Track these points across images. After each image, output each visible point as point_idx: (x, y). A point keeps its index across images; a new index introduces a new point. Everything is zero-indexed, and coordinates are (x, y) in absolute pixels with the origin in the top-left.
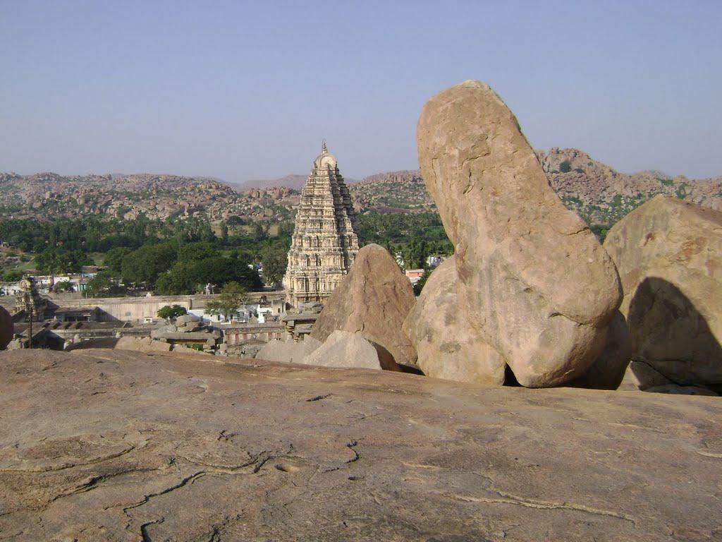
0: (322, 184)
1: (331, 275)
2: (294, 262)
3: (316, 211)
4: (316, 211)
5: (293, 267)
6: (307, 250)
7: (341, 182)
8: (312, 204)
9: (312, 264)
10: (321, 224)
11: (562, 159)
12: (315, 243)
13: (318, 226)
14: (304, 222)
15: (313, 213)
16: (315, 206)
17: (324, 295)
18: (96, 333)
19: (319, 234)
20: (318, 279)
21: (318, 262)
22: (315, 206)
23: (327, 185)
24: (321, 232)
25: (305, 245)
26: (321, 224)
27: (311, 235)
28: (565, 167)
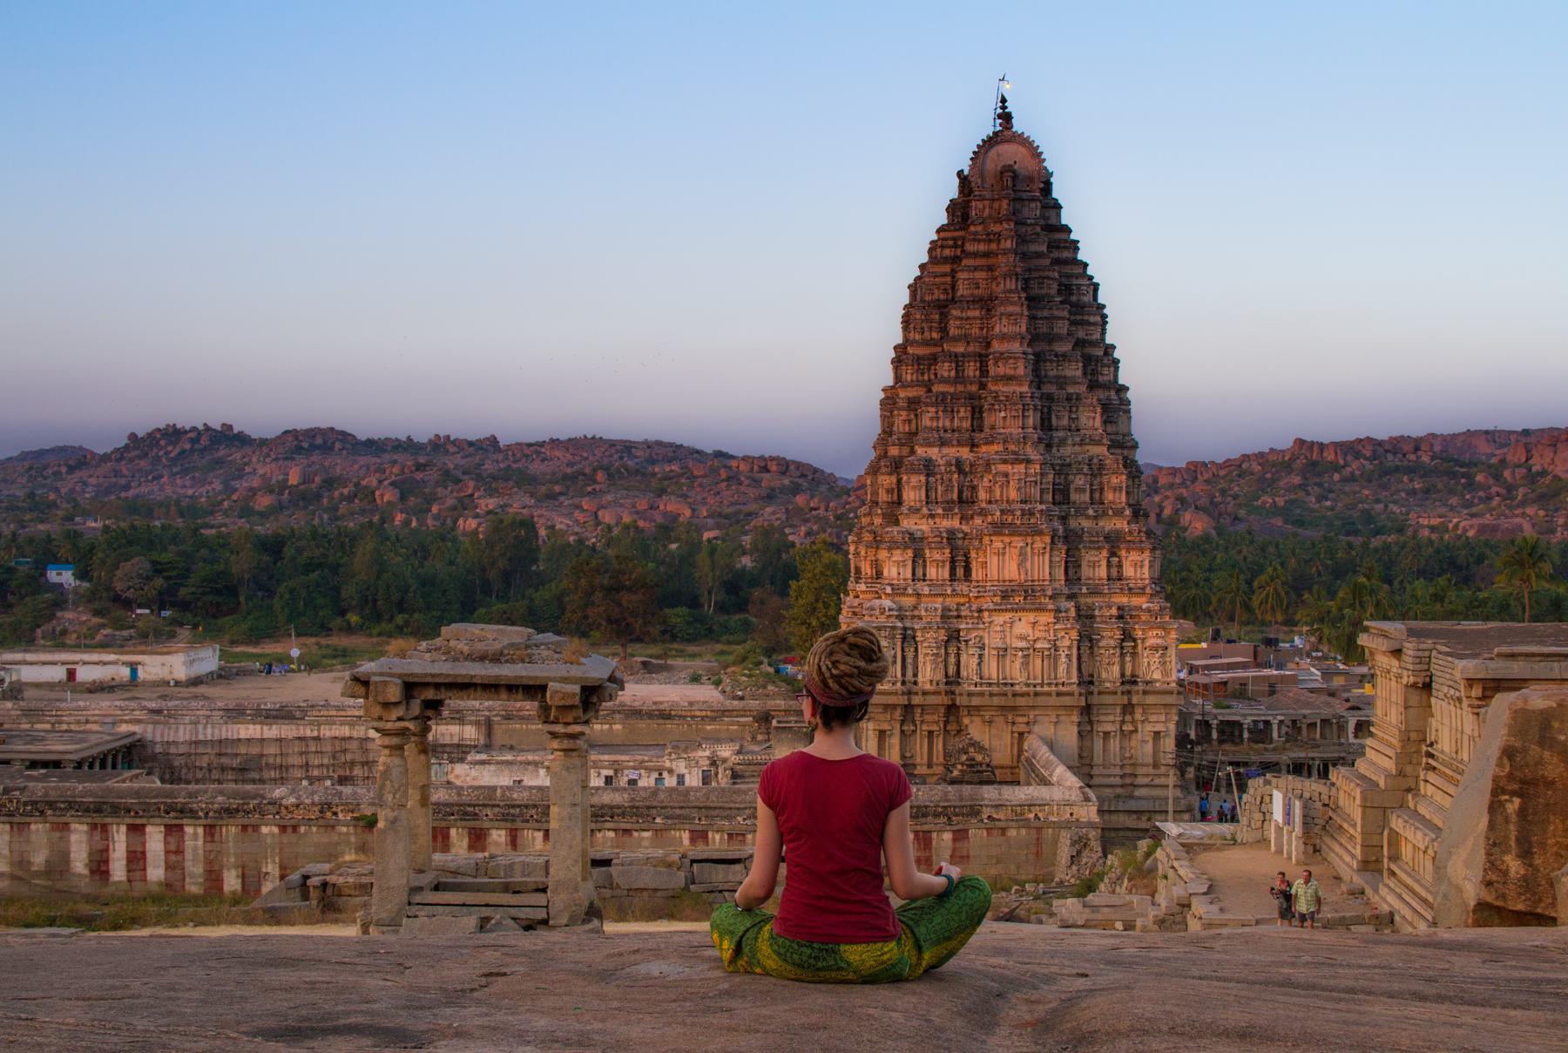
0: (986, 255)
1: (1007, 616)
2: (867, 569)
4: (957, 360)
5: (863, 587)
7: (1066, 254)
9: (932, 572)
10: (977, 413)
12: (949, 489)
13: (962, 419)
15: (945, 369)
17: (975, 701)
19: (965, 453)
21: (960, 566)
22: (956, 339)
23: (1005, 252)
24: (973, 446)
26: (977, 413)
27: (933, 452)
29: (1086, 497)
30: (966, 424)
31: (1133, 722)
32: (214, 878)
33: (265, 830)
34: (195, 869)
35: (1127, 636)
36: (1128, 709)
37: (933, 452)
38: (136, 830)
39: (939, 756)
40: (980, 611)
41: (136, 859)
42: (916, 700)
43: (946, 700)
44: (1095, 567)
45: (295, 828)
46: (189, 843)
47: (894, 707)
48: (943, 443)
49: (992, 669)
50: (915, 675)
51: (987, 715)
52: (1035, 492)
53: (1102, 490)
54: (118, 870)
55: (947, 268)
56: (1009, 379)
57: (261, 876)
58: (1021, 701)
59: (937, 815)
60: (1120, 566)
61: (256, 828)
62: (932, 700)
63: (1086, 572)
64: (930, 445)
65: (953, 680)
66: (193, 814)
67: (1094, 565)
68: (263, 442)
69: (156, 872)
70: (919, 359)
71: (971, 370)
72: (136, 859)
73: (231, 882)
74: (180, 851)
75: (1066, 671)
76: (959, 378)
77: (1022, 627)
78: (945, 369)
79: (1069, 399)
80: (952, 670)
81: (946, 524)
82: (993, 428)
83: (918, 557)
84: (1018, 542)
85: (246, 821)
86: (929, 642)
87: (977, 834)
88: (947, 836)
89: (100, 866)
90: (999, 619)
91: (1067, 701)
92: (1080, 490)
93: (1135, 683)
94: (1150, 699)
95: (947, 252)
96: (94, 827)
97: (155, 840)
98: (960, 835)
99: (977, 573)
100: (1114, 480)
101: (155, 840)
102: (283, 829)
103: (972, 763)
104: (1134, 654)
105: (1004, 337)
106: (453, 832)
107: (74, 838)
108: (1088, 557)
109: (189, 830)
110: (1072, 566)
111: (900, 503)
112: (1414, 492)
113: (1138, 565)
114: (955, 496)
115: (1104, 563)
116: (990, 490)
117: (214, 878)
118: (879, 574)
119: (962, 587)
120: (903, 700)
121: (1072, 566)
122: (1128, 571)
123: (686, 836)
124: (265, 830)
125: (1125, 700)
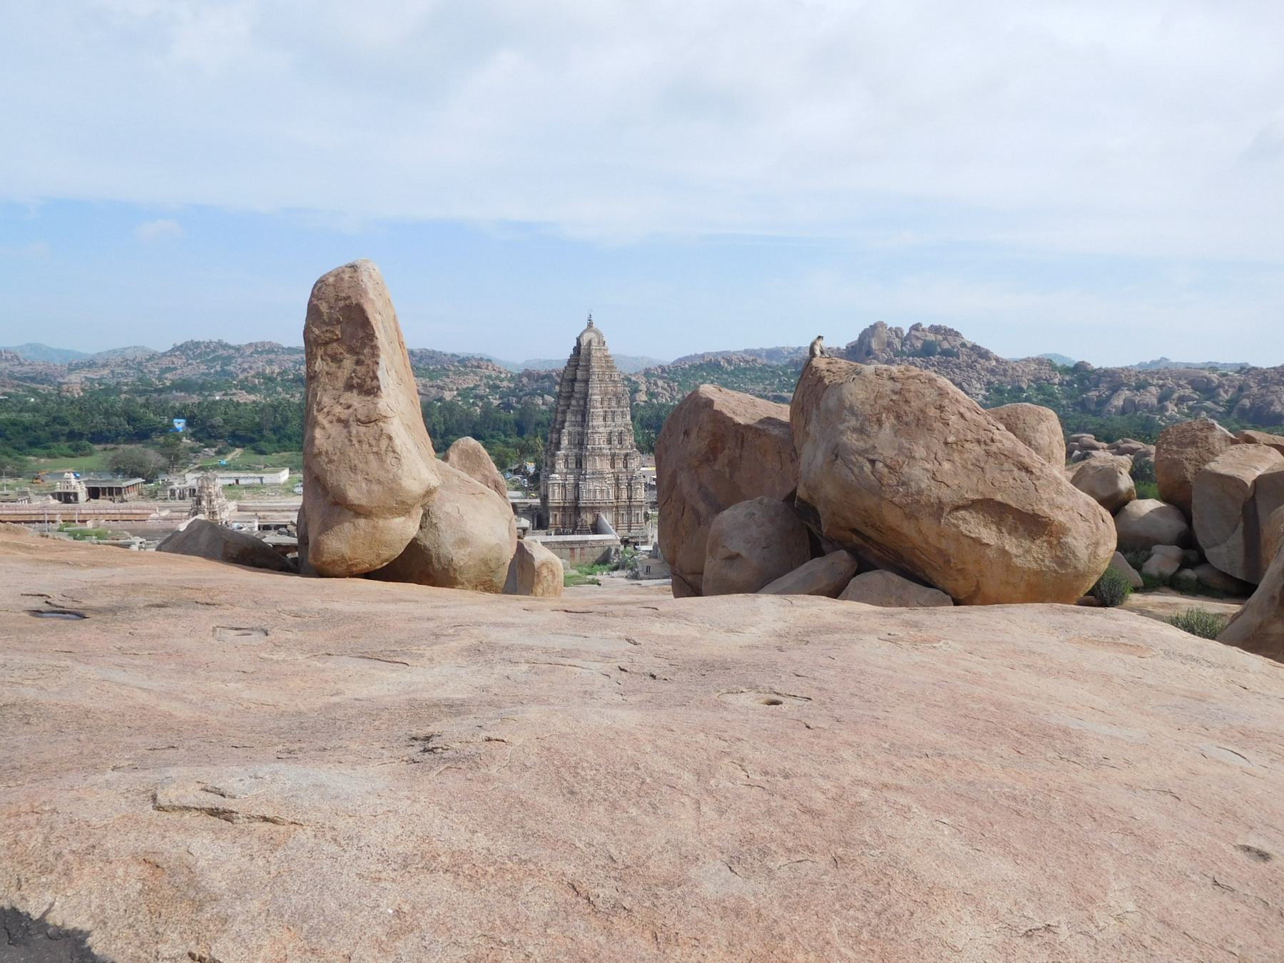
10: (583, 416)
13: (579, 418)
19: (580, 429)
21: (579, 463)
25: (565, 442)
26: (583, 416)
35: (630, 485)
36: (629, 507)
44: (620, 465)
65: (577, 498)
71: (582, 402)
75: (612, 497)
78: (574, 402)
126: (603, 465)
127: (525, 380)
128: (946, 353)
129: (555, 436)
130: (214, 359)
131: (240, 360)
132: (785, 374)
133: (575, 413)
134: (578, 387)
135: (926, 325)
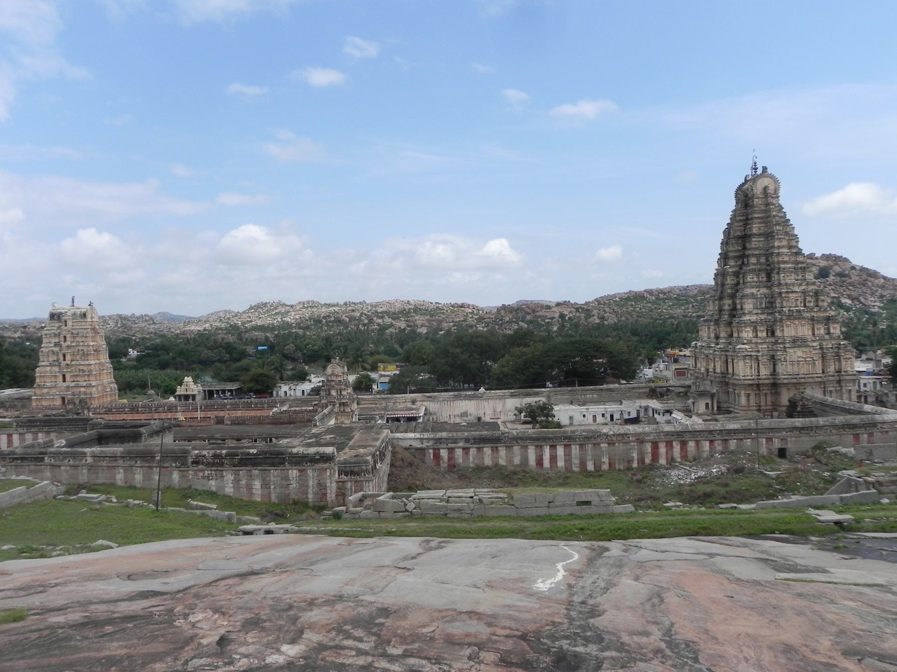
2: (723, 334)
3: (758, 256)
4: (758, 256)
6: (750, 313)
8: (745, 248)
9: (760, 334)
10: (769, 276)
11: (823, 263)
14: (736, 274)
16: (755, 249)
17: (785, 381)
18: (474, 439)
19: (765, 290)
20: (773, 357)
21: (772, 332)
25: (748, 306)
26: (769, 276)
27: (754, 291)
28: (823, 273)
29: (812, 304)
30: (765, 279)
31: (841, 386)
32: (583, 464)
33: (602, 445)
34: (576, 462)
36: (839, 382)
37: (754, 291)
38: (553, 447)
39: (769, 403)
40: (785, 347)
41: (553, 458)
42: (761, 382)
43: (772, 381)
45: (614, 444)
46: (573, 452)
47: (752, 385)
48: (759, 287)
49: (790, 369)
50: (759, 372)
51: (789, 386)
52: (799, 303)
53: (817, 301)
54: (546, 463)
55: (742, 224)
56: (784, 262)
57: (601, 463)
58: (803, 380)
59: (860, 427)
60: (828, 329)
61: (599, 444)
62: (767, 382)
63: (816, 332)
64: (752, 288)
65: (774, 373)
66: (574, 440)
67: (819, 329)
68: (292, 306)
69: (561, 463)
70: (736, 257)
71: (763, 260)
72: (553, 458)
73: (590, 467)
74: (570, 455)
76: (758, 263)
77: (799, 353)
78: (753, 260)
79: (801, 268)
80: (772, 370)
81: (763, 317)
82: (779, 280)
83: (755, 331)
84: (797, 322)
85: (595, 442)
86: (764, 360)
87: (877, 435)
88: (866, 436)
89: (540, 462)
90: (792, 351)
91: (819, 380)
92: (810, 302)
93: (840, 372)
94: (848, 378)
95: (741, 218)
96: (537, 446)
97: (560, 451)
98: (871, 435)
99: (778, 333)
100: (823, 298)
101: (560, 451)
102: (609, 444)
103: (803, 406)
104: (840, 361)
105: (779, 247)
106: (674, 444)
107: (529, 451)
108: (816, 326)
109: (573, 447)
110: (813, 330)
111: (735, 309)
112: (669, 306)
113: (835, 328)
114: (764, 306)
115: (822, 329)
116: (782, 303)
117: (583, 464)
118: (731, 336)
119: (773, 340)
120: (756, 382)
121: (813, 330)
122: (832, 331)
123: (764, 440)
124: (602, 445)
125: (837, 378)
126: (804, 331)
127: (502, 312)
128: (840, 275)
129: (727, 302)
130: (277, 314)
131: (293, 313)
132: (696, 301)
133: (757, 272)
134: (755, 243)
135: (818, 255)
